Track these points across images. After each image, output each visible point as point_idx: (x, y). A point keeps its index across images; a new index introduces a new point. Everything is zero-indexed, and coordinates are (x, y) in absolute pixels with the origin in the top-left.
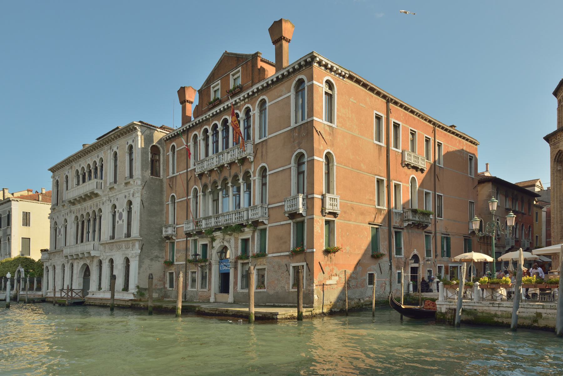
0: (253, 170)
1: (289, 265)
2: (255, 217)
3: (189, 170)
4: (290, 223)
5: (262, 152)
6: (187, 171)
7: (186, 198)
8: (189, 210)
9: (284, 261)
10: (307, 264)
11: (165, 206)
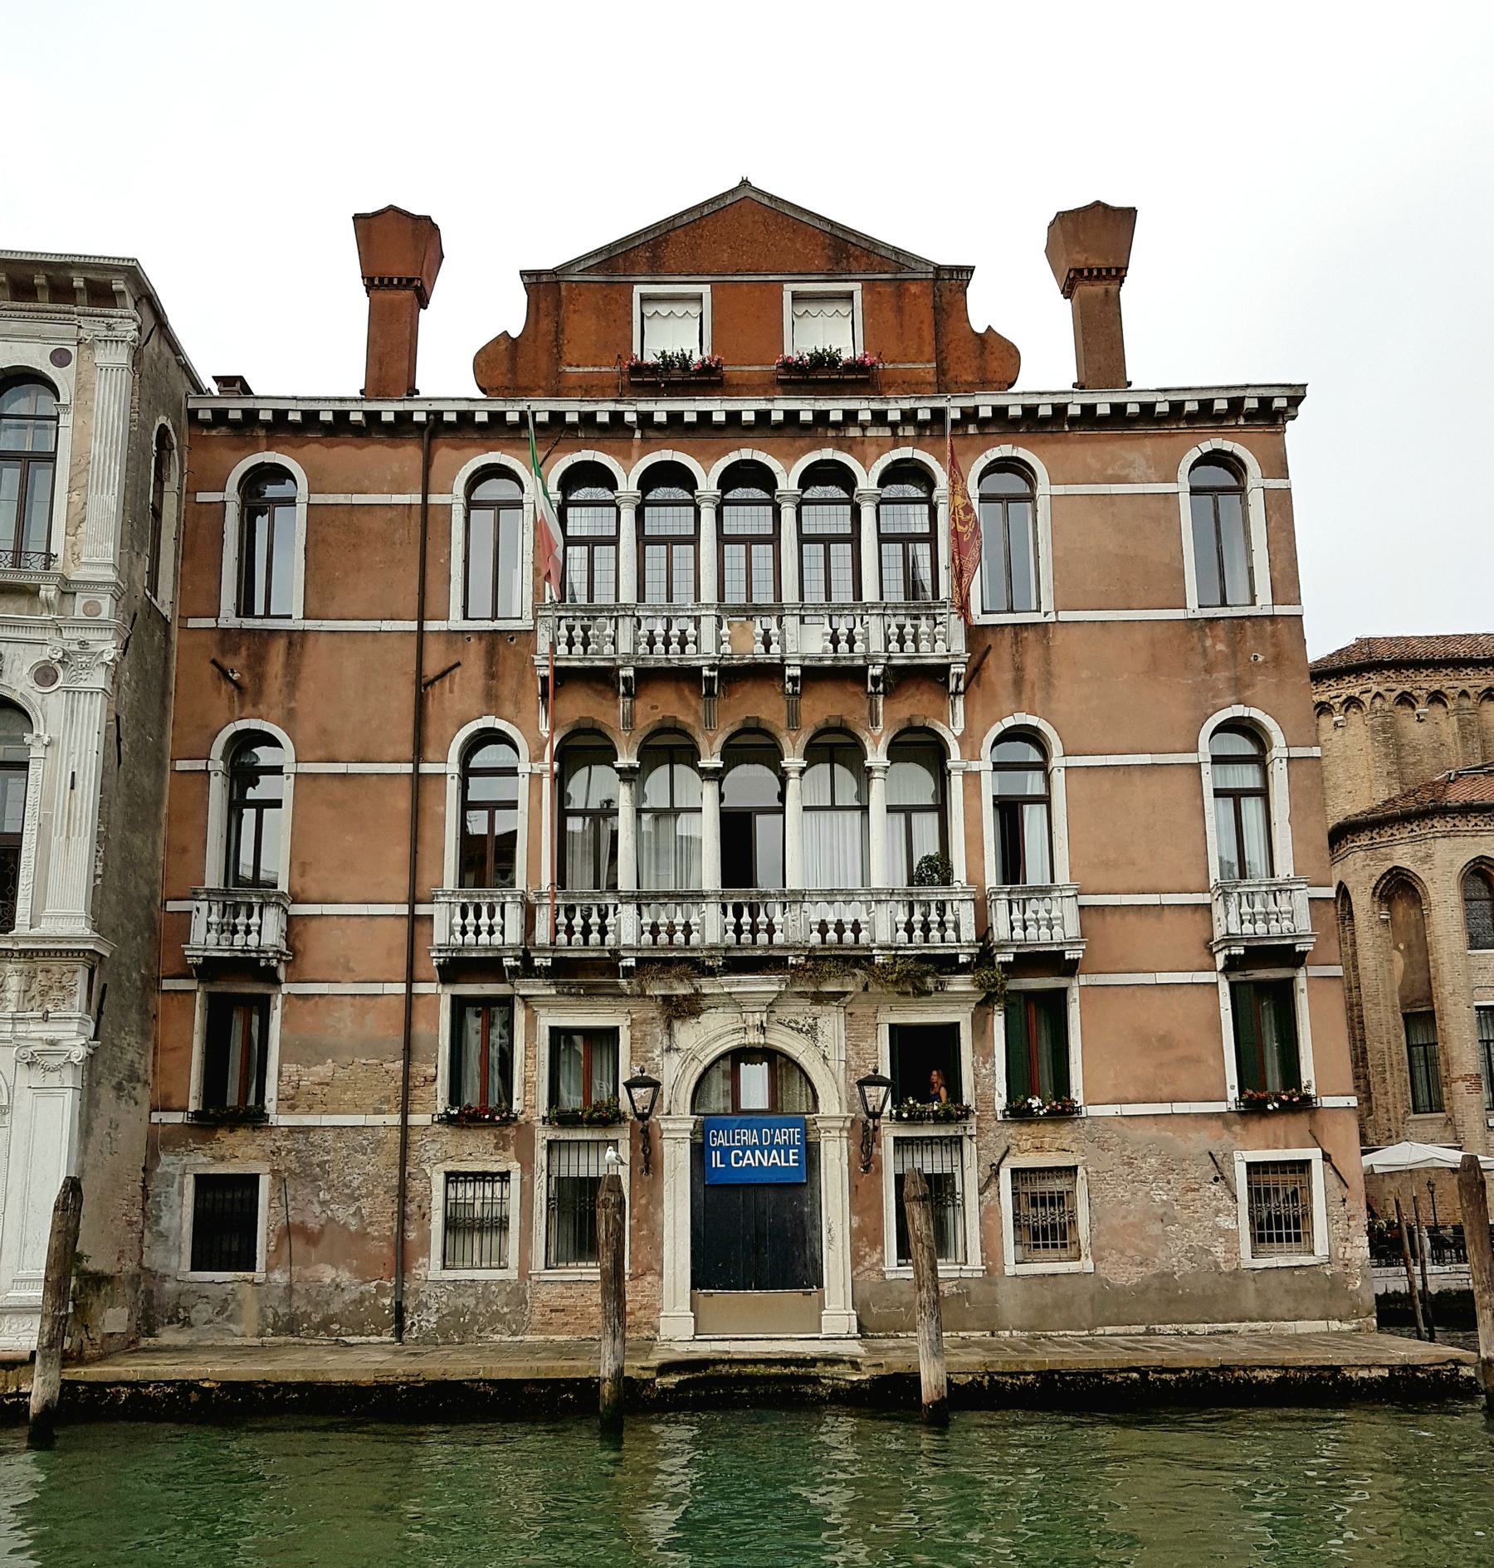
1: (1228, 1156)
2: (1039, 937)
3: (430, 626)
5: (1019, 669)
7: (408, 768)
8: (427, 833)
9: (1202, 1140)
10: (1326, 1157)
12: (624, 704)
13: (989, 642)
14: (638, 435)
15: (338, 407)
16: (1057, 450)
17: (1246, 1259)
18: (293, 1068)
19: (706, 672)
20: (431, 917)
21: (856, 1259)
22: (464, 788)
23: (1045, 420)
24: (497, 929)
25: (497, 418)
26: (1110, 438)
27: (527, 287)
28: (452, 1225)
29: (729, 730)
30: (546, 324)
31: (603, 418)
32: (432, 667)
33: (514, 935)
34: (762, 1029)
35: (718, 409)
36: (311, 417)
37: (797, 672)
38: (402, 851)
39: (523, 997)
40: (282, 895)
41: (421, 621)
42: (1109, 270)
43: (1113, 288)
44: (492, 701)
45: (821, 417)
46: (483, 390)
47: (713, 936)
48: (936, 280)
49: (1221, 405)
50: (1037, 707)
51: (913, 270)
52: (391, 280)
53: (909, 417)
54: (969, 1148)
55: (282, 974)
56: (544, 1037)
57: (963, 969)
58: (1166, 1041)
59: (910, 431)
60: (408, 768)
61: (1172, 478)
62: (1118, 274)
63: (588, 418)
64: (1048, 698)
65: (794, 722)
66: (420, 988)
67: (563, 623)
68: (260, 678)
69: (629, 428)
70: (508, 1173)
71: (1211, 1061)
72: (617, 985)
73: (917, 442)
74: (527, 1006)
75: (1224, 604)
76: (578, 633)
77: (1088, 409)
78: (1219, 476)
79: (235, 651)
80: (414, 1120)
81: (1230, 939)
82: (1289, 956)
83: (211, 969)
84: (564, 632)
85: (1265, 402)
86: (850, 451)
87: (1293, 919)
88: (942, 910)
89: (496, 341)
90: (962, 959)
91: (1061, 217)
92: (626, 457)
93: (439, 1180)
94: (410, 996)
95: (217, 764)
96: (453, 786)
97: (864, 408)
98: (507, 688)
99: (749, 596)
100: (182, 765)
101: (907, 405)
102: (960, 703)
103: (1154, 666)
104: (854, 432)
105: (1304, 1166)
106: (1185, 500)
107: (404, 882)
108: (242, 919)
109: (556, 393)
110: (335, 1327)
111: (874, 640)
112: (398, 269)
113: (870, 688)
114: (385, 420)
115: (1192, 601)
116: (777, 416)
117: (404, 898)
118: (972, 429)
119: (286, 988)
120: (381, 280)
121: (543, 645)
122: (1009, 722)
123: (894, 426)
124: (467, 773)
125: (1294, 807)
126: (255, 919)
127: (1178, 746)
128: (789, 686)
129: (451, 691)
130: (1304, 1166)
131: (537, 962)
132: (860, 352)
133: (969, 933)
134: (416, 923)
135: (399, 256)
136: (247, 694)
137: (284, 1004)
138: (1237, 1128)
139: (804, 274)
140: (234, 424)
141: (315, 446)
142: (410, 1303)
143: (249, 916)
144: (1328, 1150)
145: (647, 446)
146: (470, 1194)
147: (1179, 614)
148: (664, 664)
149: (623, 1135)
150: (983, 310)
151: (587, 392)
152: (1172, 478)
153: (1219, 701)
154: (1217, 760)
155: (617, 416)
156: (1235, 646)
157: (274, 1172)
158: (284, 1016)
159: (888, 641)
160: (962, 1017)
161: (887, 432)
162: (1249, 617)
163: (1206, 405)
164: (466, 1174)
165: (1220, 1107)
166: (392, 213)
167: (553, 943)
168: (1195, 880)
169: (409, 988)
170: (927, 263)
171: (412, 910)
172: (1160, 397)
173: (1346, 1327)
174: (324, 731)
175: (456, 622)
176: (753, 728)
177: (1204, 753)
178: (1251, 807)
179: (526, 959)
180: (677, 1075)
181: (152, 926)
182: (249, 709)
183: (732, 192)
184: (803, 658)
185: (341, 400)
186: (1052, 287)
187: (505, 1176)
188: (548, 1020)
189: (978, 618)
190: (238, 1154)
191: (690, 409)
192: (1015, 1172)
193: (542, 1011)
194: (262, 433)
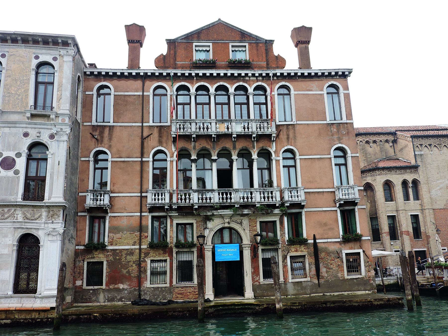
0: (274, 149)
1: (341, 251)
2: (295, 199)
3: (144, 124)
4: (337, 210)
5: (288, 135)
6: (142, 126)
7: (140, 159)
8: (145, 176)
10: (364, 251)
11: (79, 162)
12: (193, 144)
13: (281, 128)
14: (195, 78)
15: (122, 71)
16: (296, 83)
17: (346, 277)
18: (112, 234)
19: (213, 136)
20: (146, 197)
21: (253, 279)
22: (153, 164)
23: (293, 76)
24: (163, 199)
25: (161, 74)
26: (306, 81)
27: (167, 43)
28: (152, 273)
29: (219, 150)
30: (172, 52)
31: (187, 74)
32: (145, 134)
33: (167, 201)
34: (229, 223)
35: (215, 72)
36: (115, 74)
37: (235, 136)
38: (138, 180)
39: (170, 216)
40: (108, 191)
41: (142, 123)
42: (306, 41)
43: (307, 45)
44: (160, 143)
45: (240, 75)
46: (157, 67)
47: (217, 200)
48: (266, 43)
49: (333, 73)
50: (293, 144)
51: (260, 41)
52: (134, 41)
53: (260, 75)
54: (280, 251)
55: (109, 211)
56: (175, 225)
57: (278, 207)
58: (325, 224)
59: (261, 78)
60: (140, 159)
61: (322, 90)
62: (308, 42)
63: (183, 74)
64: (295, 142)
65: (234, 148)
66: (143, 214)
67: (178, 124)
68: (102, 137)
69: (193, 77)
70: (166, 260)
71: (336, 229)
72: (193, 213)
73: (262, 81)
74: (171, 218)
75: (335, 120)
76: (182, 126)
77: (303, 74)
78: (333, 90)
79: (96, 130)
80: (142, 247)
81: (340, 200)
82: (354, 203)
83: (91, 210)
84: (178, 126)
85: (343, 73)
86: (246, 83)
87: (355, 194)
88: (272, 194)
89: (160, 56)
90: (277, 205)
91: (295, 29)
92: (192, 84)
93: (149, 262)
94: (141, 216)
95: (92, 159)
96: (151, 164)
97: (250, 73)
98: (164, 139)
99: (222, 118)
100: (83, 159)
101: (260, 72)
102: (274, 143)
103: (320, 134)
104: (247, 78)
105: (359, 254)
106: (325, 95)
107: (139, 188)
108: (99, 197)
109: (175, 68)
110: (123, 299)
111: (254, 128)
112: (136, 38)
113: (253, 140)
114: (133, 76)
115: (328, 119)
116: (229, 74)
117: (139, 191)
118: (275, 78)
119: (109, 214)
120: (132, 41)
121: (173, 129)
122: (286, 148)
123: (257, 77)
124: (154, 160)
125: (353, 168)
126: (102, 197)
127: (326, 153)
128: (233, 139)
129: (150, 140)
130: (359, 254)
131: (173, 207)
132: (248, 59)
133: (278, 199)
134: (142, 198)
135: (135, 36)
136: (99, 141)
137: (109, 219)
138: (343, 245)
139: (234, 41)
140: (96, 75)
141: (115, 81)
142: (142, 293)
143: (101, 197)
144: (364, 250)
145: (198, 81)
146: (157, 265)
147: (325, 122)
148: (203, 134)
149: (195, 250)
150: (277, 50)
151: (182, 68)
152: (322, 90)
153: (335, 143)
154: (335, 157)
155: (190, 74)
156: (338, 130)
157: (107, 261)
158: (109, 221)
159: (257, 128)
160: (277, 219)
161: (255, 78)
162: (341, 123)
163: (330, 73)
164: (156, 260)
165: (339, 240)
166: (135, 25)
167: (177, 202)
168: (331, 186)
169: (141, 214)
170: (264, 39)
171: (141, 194)
172: (319, 71)
173: (370, 292)
174: (118, 151)
175: (151, 124)
176: (224, 149)
177: (332, 155)
178: (343, 168)
179: (171, 206)
180: (209, 234)
181: (76, 199)
182: (100, 145)
183: (217, 21)
184: (237, 132)
185: (122, 70)
186: (292, 45)
187: (165, 261)
188: (175, 222)
189: (278, 123)
190: (99, 257)
191: (208, 72)
192: (291, 257)
193: (174, 219)
194: (102, 77)
